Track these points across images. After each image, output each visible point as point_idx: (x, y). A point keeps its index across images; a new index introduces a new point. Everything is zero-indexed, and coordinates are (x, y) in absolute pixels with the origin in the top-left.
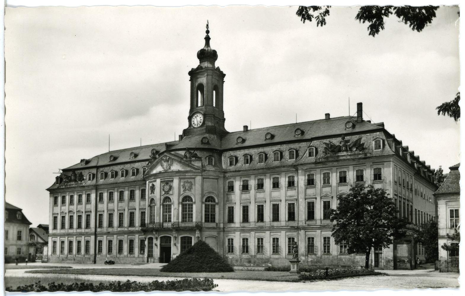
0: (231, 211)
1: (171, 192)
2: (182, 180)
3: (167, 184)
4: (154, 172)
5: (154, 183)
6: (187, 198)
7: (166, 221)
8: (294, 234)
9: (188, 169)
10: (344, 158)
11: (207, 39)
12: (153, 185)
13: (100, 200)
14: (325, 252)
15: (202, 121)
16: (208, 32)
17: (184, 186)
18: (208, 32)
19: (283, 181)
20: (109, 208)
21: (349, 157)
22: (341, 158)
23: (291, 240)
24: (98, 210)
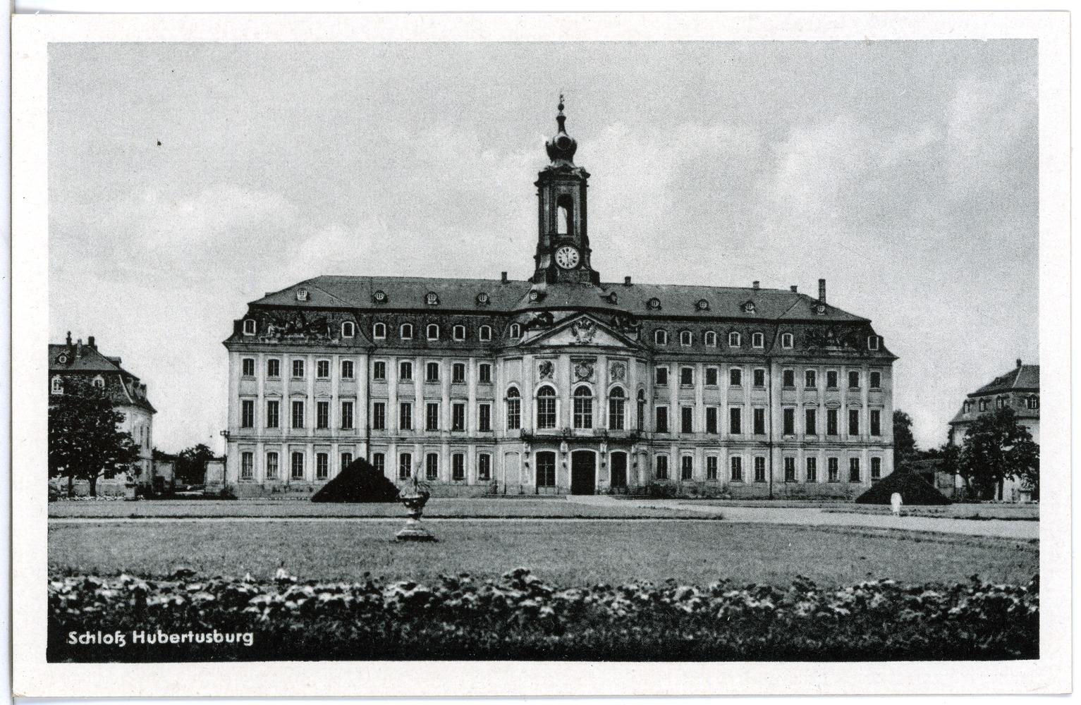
0: (662, 413)
1: (593, 378)
2: (610, 362)
3: (584, 365)
4: (554, 341)
5: (552, 361)
6: (617, 392)
7: (580, 426)
8: (764, 453)
9: (620, 344)
10: (835, 354)
11: (561, 120)
12: (549, 364)
13: (376, 375)
14: (809, 477)
15: (577, 260)
16: (561, 107)
17: (613, 371)
18: (561, 107)
19: (747, 378)
20: (401, 393)
21: (841, 354)
22: (831, 354)
23: (759, 462)
24: (372, 394)
